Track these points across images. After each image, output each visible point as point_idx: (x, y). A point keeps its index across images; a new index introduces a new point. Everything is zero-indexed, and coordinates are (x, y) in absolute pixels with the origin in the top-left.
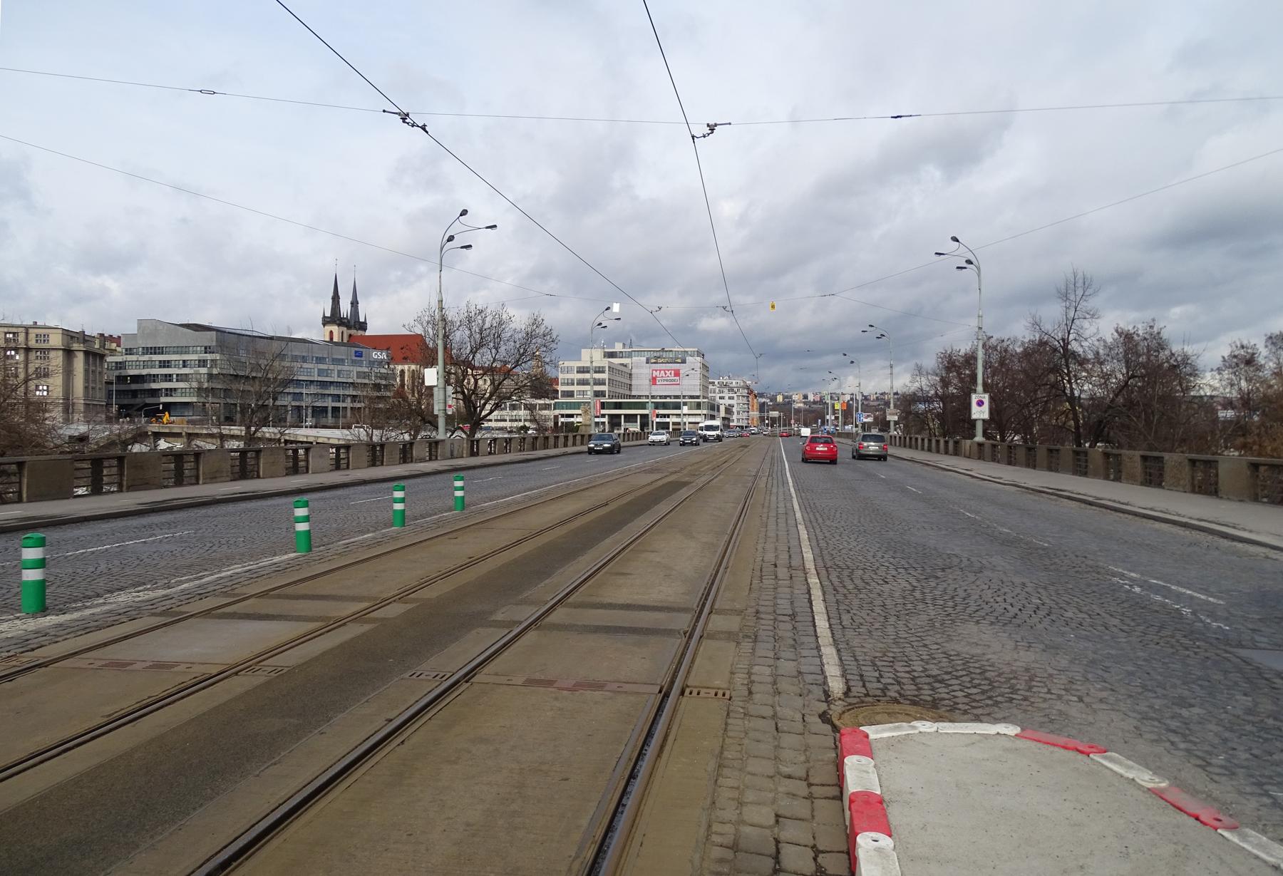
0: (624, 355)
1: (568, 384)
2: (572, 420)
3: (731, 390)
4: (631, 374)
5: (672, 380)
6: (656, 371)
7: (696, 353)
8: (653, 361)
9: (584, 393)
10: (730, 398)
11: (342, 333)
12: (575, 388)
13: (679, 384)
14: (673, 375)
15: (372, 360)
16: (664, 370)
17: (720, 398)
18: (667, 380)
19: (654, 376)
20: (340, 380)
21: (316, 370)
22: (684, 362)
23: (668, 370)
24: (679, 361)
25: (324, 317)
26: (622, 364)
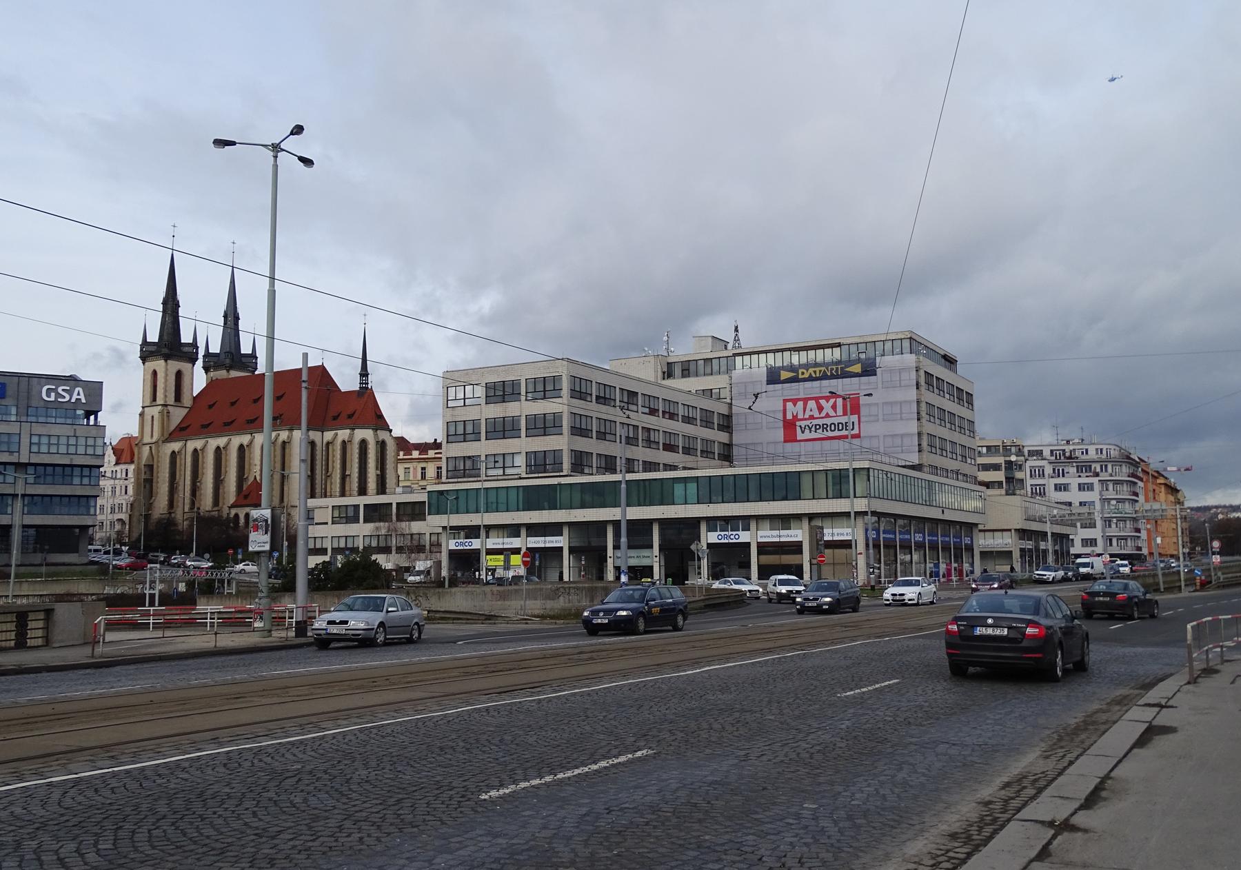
0: (716, 368)
2: (476, 544)
3: (1084, 468)
4: (728, 417)
5: (837, 426)
6: (795, 402)
7: (906, 344)
8: (785, 375)
9: (501, 460)
10: (1081, 487)
11: (155, 373)
12: (482, 448)
13: (857, 436)
14: (840, 411)
15: (42, 404)
16: (817, 399)
17: (1058, 488)
18: (824, 427)
19: (789, 417)
22: (869, 370)
23: (827, 399)
24: (857, 368)
25: (145, 342)
26: (708, 393)
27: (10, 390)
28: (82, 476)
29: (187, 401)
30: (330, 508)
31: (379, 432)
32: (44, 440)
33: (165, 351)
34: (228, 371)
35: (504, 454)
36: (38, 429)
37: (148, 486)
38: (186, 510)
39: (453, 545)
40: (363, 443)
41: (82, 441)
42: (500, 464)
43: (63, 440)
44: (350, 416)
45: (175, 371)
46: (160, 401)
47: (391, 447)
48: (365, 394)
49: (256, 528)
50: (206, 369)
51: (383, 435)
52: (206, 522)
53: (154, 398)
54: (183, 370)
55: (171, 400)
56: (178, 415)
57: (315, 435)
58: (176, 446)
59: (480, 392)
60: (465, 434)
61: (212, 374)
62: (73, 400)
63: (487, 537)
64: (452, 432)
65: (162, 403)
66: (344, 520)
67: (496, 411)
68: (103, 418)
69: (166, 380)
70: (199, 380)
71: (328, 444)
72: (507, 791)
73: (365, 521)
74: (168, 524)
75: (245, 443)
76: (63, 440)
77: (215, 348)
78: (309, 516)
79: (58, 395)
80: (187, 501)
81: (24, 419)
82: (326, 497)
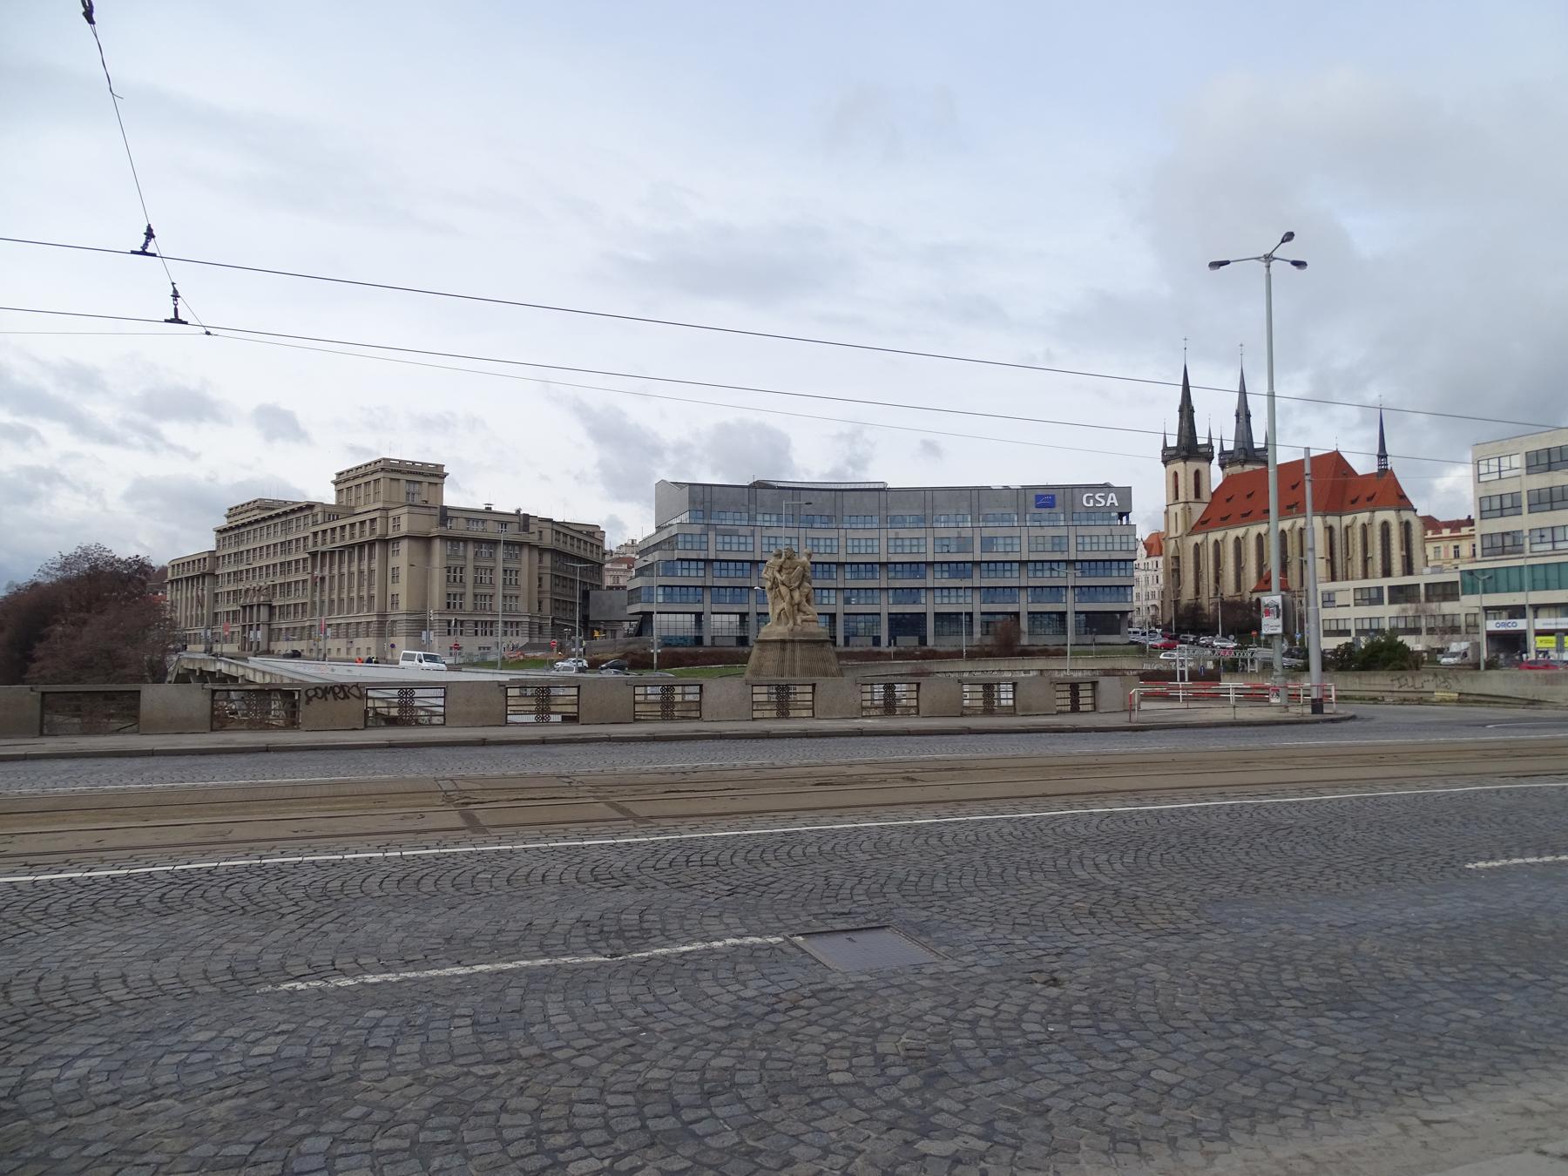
1: (1502, 512)
2: (1521, 624)
11: (1176, 474)
12: (1524, 522)
15: (1084, 509)
20: (986, 557)
21: (930, 541)
25: (1166, 448)
27: (1058, 501)
28: (1119, 569)
29: (1206, 497)
30: (1352, 591)
31: (1402, 512)
32: (1087, 540)
33: (1184, 453)
34: (1243, 466)
35: (1553, 528)
36: (1081, 531)
37: (1176, 576)
38: (1211, 596)
39: (1492, 625)
40: (1385, 526)
41: (1117, 539)
42: (1548, 538)
43: (1102, 540)
44: (1370, 499)
45: (1193, 471)
46: (1182, 498)
47: (1416, 529)
48: (1385, 473)
49: (1268, 613)
50: (1222, 466)
51: (1406, 515)
52: (1229, 607)
53: (1177, 498)
54: (1201, 469)
55: (1192, 497)
56: (1199, 510)
57: (1333, 520)
58: (1198, 538)
59: (1518, 461)
60: (1502, 509)
61: (1229, 470)
62: (1108, 505)
63: (1536, 617)
64: (1486, 507)
65: (1184, 500)
66: (1367, 602)
67: (1541, 481)
68: (1133, 517)
69: (1186, 480)
70: (1216, 475)
71: (1347, 527)
72: (1496, 864)
73: (1391, 602)
74: (1195, 609)
75: (1263, 532)
76: (1102, 540)
77: (1229, 446)
78: (1329, 600)
79: (1096, 501)
80: (1212, 587)
81: (1070, 523)
82: (1347, 579)
